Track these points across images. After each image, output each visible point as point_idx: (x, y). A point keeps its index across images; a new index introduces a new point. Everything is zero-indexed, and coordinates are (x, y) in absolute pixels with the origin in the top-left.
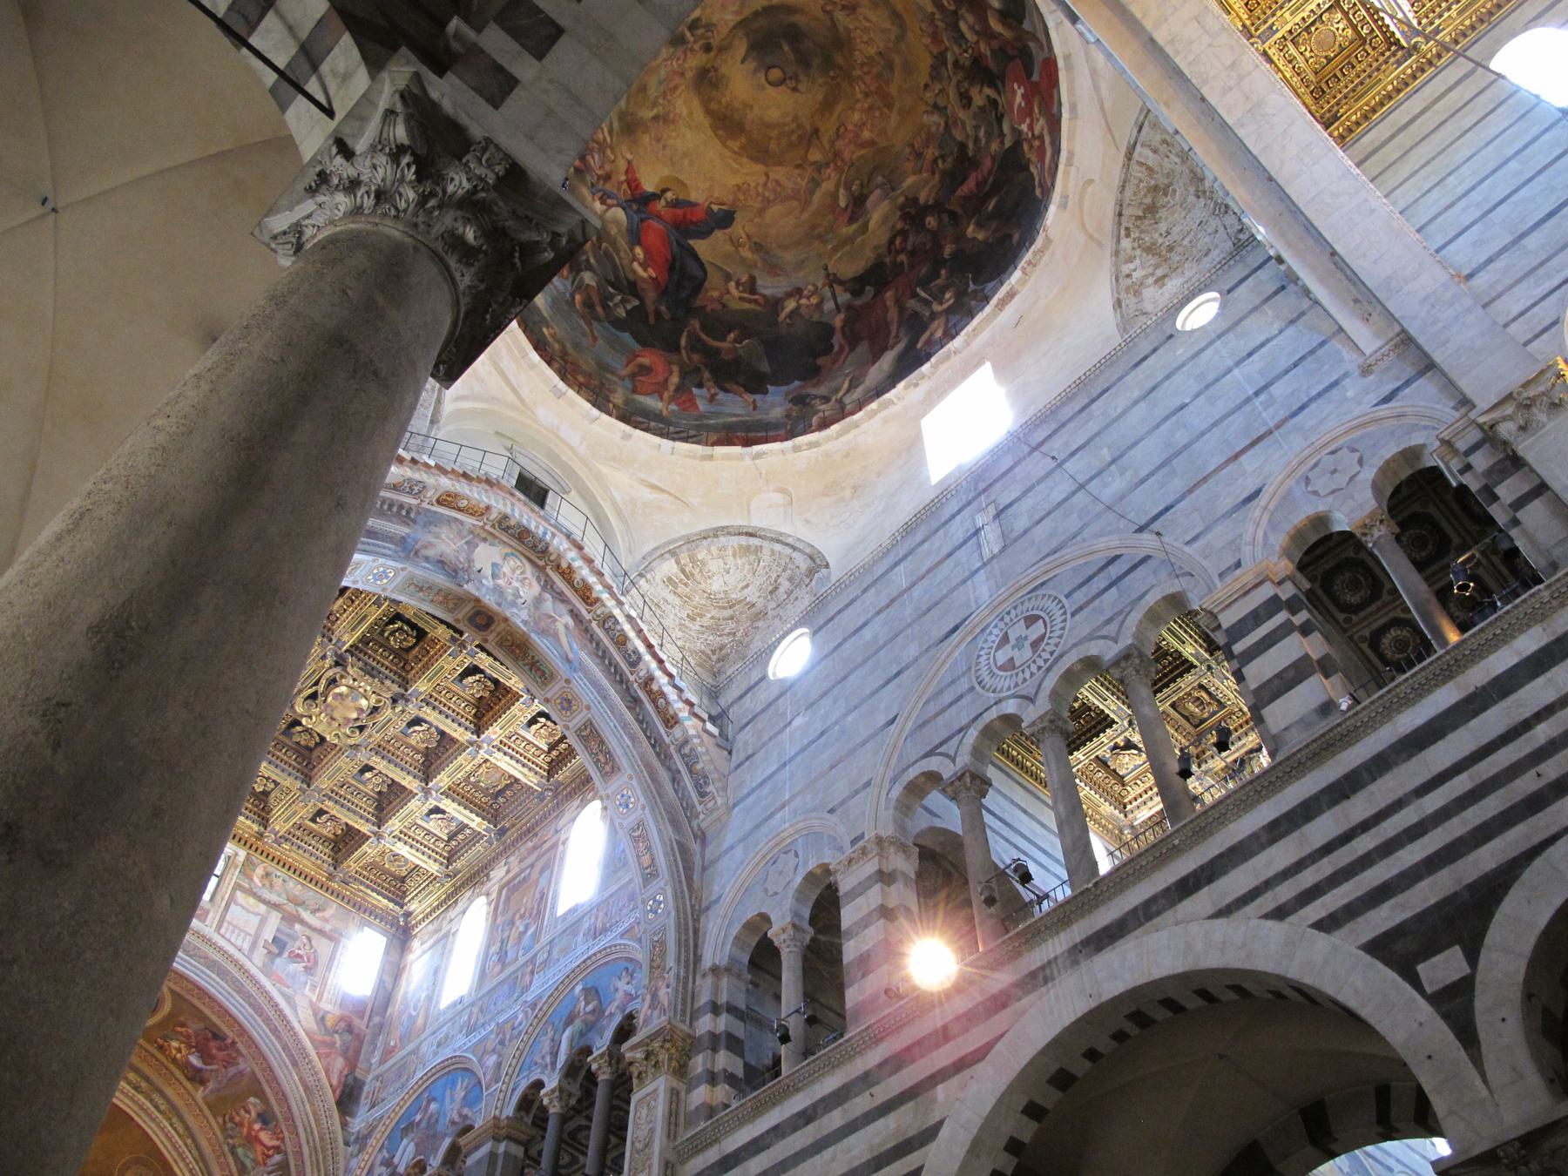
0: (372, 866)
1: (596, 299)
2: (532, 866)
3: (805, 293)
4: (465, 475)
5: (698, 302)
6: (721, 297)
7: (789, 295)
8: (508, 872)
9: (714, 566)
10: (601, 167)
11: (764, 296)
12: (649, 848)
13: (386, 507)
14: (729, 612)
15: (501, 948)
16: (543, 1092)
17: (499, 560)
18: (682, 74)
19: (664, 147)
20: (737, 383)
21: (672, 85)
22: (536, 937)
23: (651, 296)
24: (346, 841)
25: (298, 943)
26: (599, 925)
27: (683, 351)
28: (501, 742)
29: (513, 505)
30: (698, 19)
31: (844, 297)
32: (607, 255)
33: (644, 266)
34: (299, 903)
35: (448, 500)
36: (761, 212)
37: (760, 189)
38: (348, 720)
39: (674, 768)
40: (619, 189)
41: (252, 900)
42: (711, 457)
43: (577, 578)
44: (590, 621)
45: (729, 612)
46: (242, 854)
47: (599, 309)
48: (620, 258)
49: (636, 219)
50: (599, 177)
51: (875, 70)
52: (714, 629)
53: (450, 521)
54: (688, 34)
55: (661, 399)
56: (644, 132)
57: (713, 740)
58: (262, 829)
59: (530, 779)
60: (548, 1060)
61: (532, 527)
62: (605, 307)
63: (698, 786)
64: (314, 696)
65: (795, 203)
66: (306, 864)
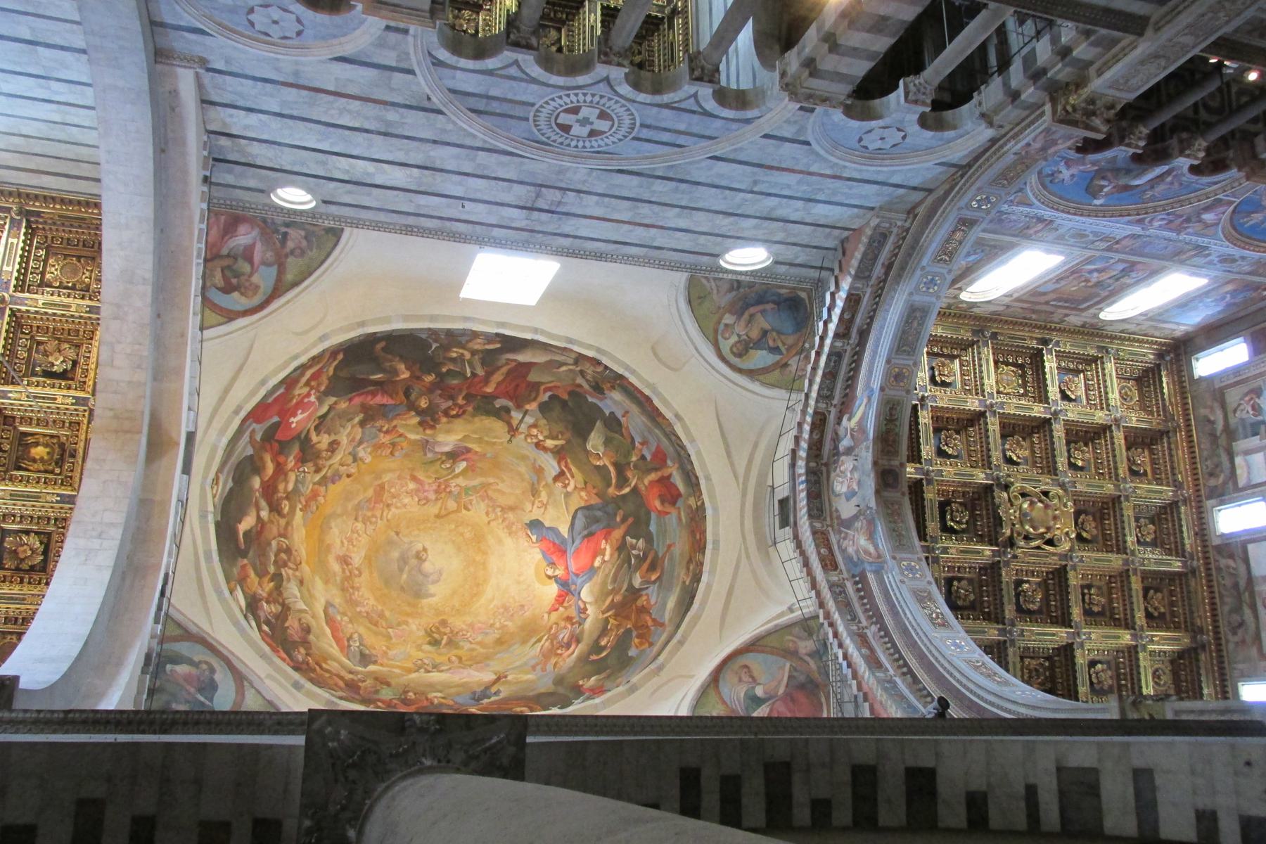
0: (1144, 406)
2: (1047, 303)
3: (535, 441)
5: (595, 501)
6: (582, 489)
7: (545, 449)
8: (1067, 315)
10: (565, 628)
11: (559, 463)
12: (948, 241)
15: (1123, 277)
16: (1196, 162)
22: (1089, 261)
23: (617, 534)
24: (1137, 440)
25: (1244, 415)
26: (1040, 226)
28: (977, 394)
30: (430, 643)
31: (516, 416)
33: (603, 553)
34: (1213, 437)
35: (829, 564)
38: (1047, 507)
39: (883, 271)
40: (570, 606)
41: (1239, 472)
42: (677, 416)
44: (835, 406)
46: (1209, 503)
48: (610, 570)
49: (579, 581)
50: (572, 624)
51: (369, 514)
53: (843, 551)
54: (444, 642)
58: (1180, 504)
59: (988, 353)
60: (1169, 179)
64: (1050, 542)
65: (490, 493)
66: (1182, 454)
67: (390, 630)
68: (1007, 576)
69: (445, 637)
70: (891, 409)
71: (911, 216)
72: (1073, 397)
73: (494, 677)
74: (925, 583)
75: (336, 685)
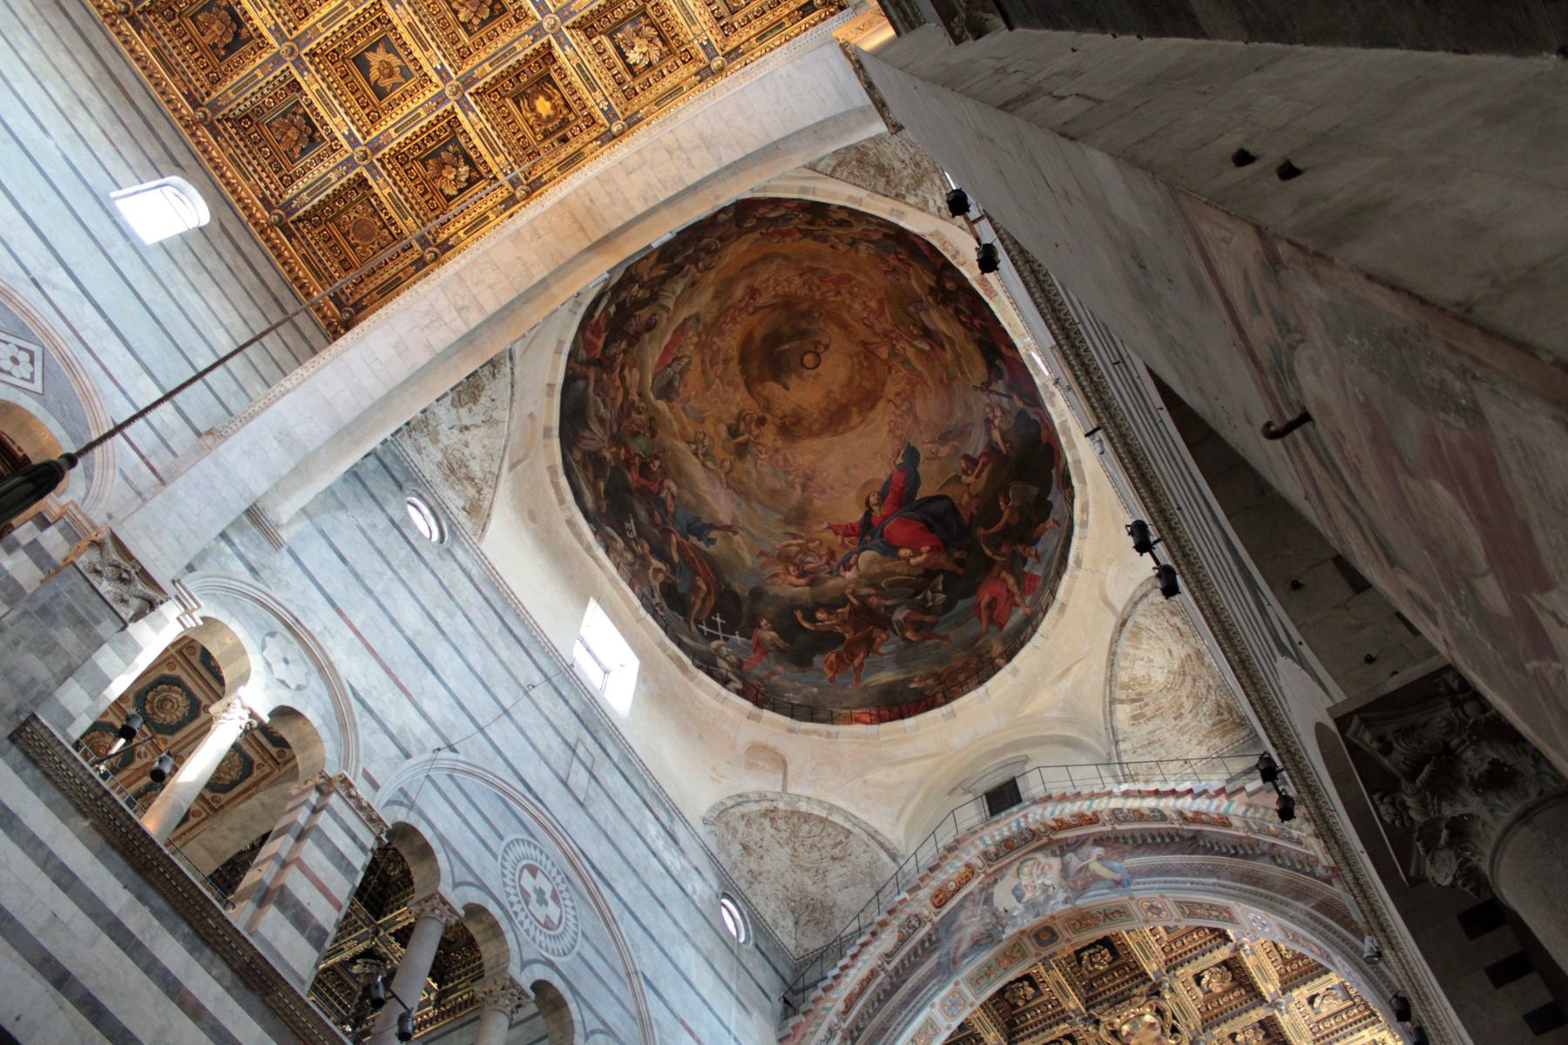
1: (917, 617)
3: (990, 416)
4: (932, 869)
6: (970, 494)
7: (989, 432)
9: (1140, 670)
11: (983, 454)
12: (1304, 938)
13: (913, 959)
14: (1189, 678)
17: (1015, 882)
18: (776, 450)
19: (832, 488)
20: (1037, 525)
21: (781, 463)
23: (942, 560)
27: (996, 558)
29: (981, 838)
30: (729, 428)
31: (1000, 386)
32: (892, 585)
33: (917, 553)
35: (940, 900)
36: (916, 420)
37: (898, 412)
43: (1067, 818)
45: (1189, 678)
47: (928, 618)
48: (901, 574)
49: (877, 541)
50: (828, 563)
51: (817, 282)
52: (1198, 701)
54: (740, 439)
55: (1017, 605)
56: (811, 504)
57: (1264, 792)
61: (1006, 833)
62: (927, 611)
63: (1290, 839)
65: (918, 387)
67: (718, 381)
68: (1063, 1029)
69: (747, 436)
70: (1118, 912)
71: (1330, 873)
72: (1316, 1005)
73: (727, 522)
74: (945, 1024)
75: (613, 400)
